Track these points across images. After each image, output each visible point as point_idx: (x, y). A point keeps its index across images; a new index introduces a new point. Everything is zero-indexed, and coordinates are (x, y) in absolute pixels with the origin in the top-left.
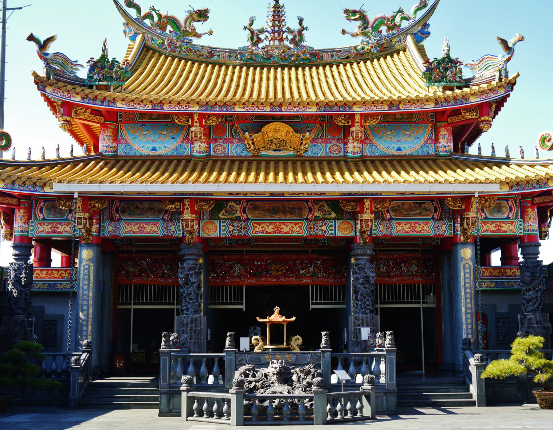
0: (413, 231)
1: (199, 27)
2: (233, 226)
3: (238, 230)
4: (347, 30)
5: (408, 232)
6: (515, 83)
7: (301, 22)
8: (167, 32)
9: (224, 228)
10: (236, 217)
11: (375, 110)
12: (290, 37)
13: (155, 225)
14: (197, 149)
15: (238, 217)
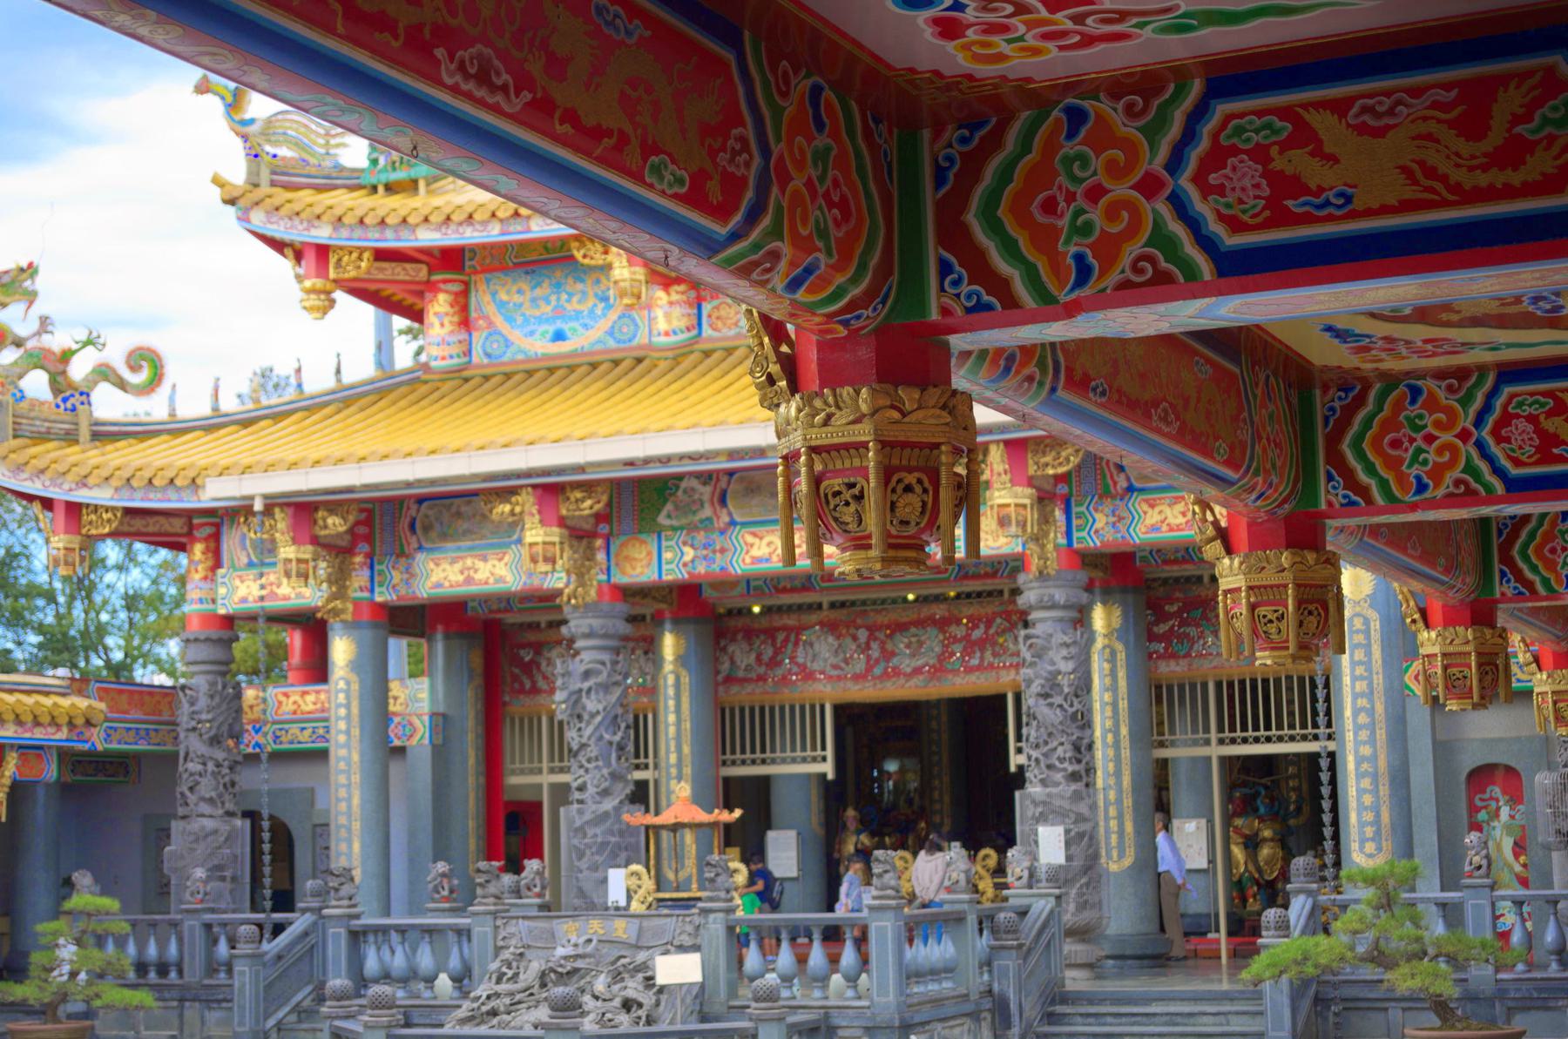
2: (692, 546)
3: (705, 558)
5: (1179, 528)
10: (701, 521)
14: (662, 325)
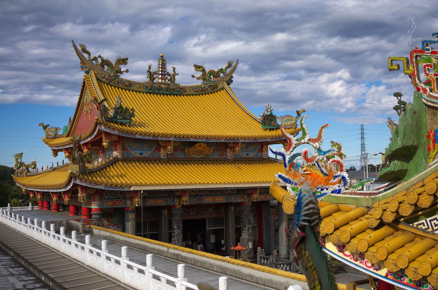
1: (123, 68)
4: (195, 76)
7: (174, 69)
8: (105, 69)
12: (169, 78)
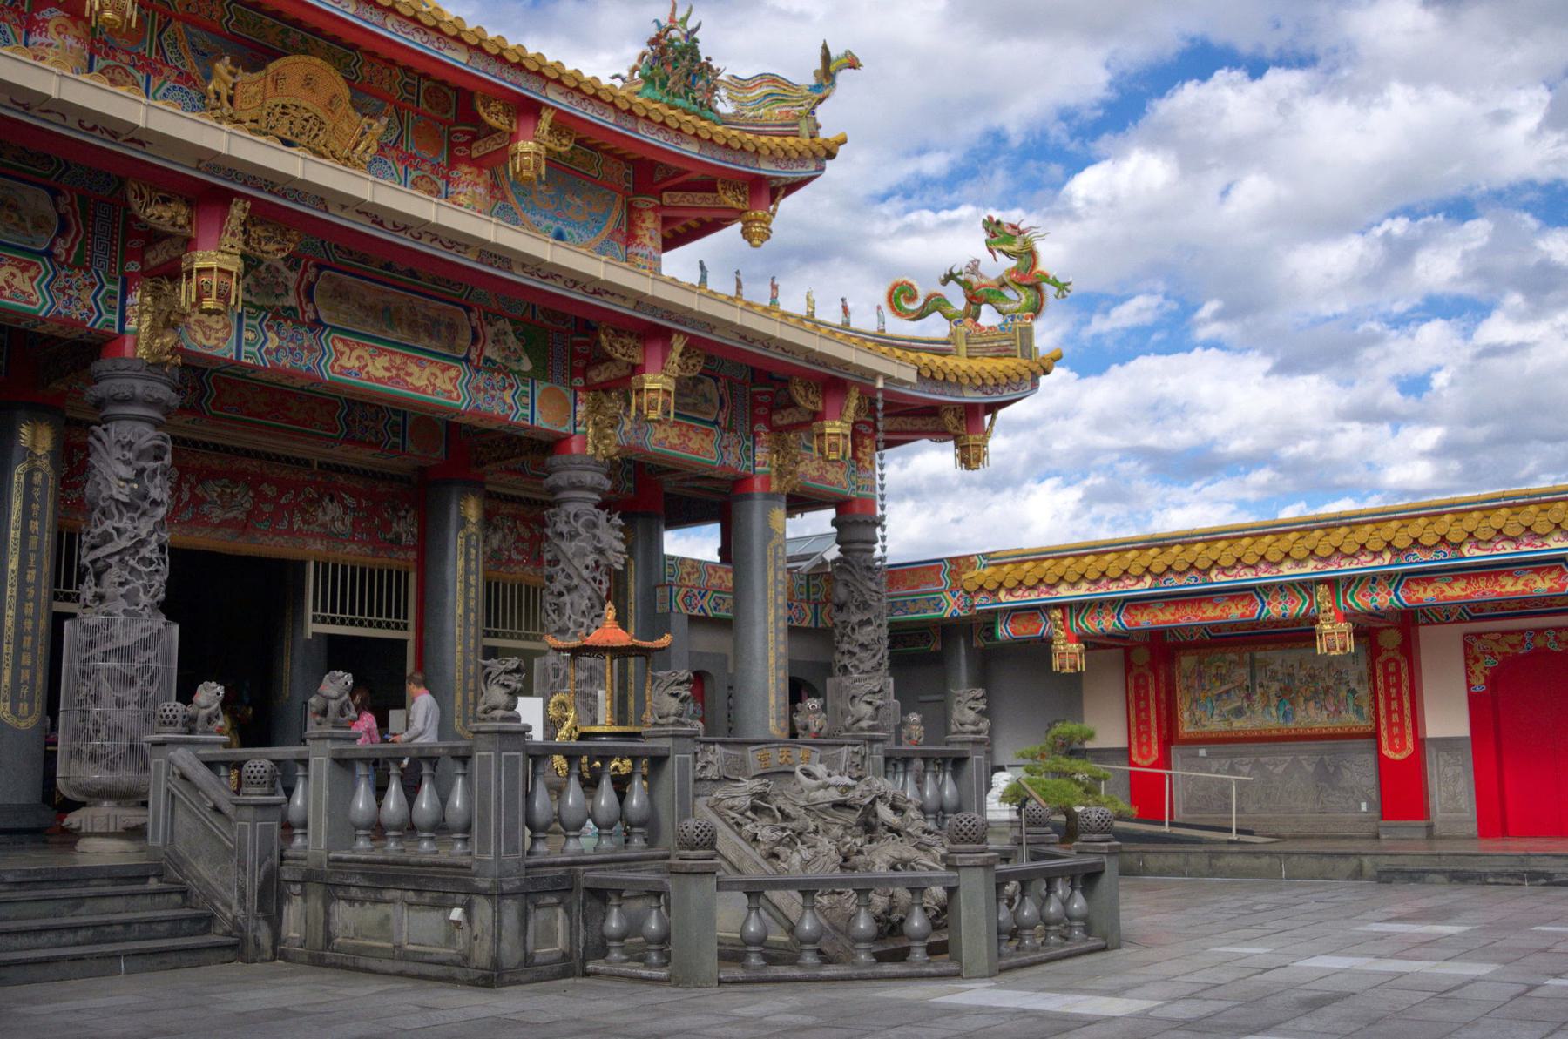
0: (684, 447)
2: (278, 334)
3: (292, 351)
6: (831, 155)
9: (251, 336)
11: (588, 113)
13: (24, 270)
15: (291, 308)
